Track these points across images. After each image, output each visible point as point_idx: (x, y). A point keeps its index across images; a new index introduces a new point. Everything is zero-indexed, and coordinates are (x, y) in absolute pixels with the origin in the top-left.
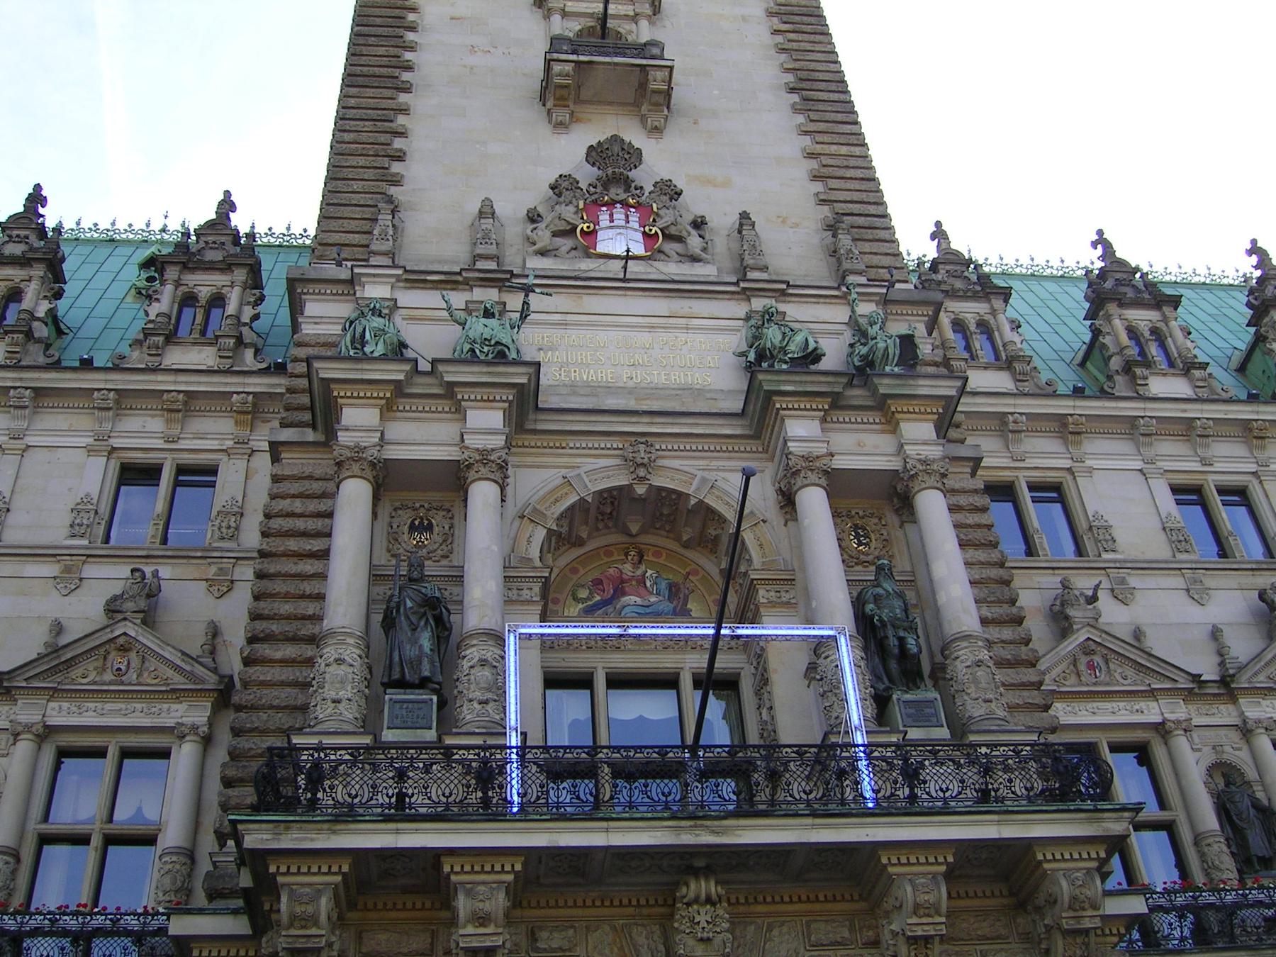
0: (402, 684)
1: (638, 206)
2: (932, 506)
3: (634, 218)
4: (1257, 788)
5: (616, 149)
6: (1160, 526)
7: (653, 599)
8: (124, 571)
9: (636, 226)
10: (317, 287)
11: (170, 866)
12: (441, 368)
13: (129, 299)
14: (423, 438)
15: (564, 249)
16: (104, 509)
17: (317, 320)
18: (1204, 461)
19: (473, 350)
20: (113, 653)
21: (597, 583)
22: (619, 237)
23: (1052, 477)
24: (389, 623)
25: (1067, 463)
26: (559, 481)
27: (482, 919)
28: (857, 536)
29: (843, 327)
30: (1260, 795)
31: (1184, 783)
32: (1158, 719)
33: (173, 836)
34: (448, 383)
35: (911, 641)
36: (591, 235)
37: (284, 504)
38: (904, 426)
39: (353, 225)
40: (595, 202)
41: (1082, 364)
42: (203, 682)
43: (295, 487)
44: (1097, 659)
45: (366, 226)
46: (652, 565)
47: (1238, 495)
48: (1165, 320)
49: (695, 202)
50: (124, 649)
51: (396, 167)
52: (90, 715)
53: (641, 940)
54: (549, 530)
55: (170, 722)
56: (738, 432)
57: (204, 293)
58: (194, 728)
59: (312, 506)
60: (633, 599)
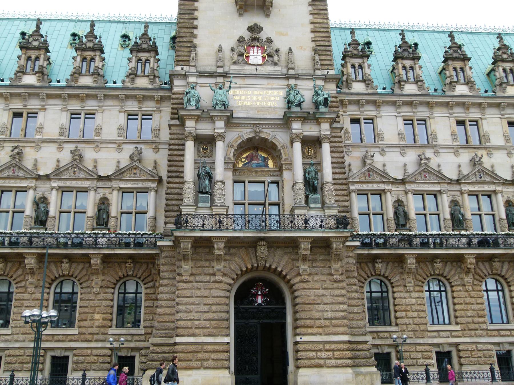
1: (262, 47)
2: (326, 147)
3: (260, 51)
5: (256, 27)
6: (397, 133)
9: (260, 54)
13: (120, 49)
14: (205, 129)
15: (241, 60)
16: (125, 128)
17: (178, 86)
18: (414, 113)
21: (247, 157)
22: (256, 56)
23: (371, 117)
24: (199, 177)
25: (375, 114)
26: (237, 136)
27: (219, 249)
28: (309, 151)
30: (406, 209)
32: (384, 189)
33: (151, 213)
35: (316, 183)
36: (248, 57)
37: (173, 142)
38: (322, 124)
39: (184, 54)
40: (249, 45)
42: (155, 177)
43: (175, 137)
44: (371, 173)
45: (188, 54)
49: (277, 44)
50: (135, 169)
51: (195, 32)
52: (129, 185)
54: (235, 149)
55: (148, 186)
57: (144, 59)
58: (154, 188)
59: (179, 142)
60: (255, 162)
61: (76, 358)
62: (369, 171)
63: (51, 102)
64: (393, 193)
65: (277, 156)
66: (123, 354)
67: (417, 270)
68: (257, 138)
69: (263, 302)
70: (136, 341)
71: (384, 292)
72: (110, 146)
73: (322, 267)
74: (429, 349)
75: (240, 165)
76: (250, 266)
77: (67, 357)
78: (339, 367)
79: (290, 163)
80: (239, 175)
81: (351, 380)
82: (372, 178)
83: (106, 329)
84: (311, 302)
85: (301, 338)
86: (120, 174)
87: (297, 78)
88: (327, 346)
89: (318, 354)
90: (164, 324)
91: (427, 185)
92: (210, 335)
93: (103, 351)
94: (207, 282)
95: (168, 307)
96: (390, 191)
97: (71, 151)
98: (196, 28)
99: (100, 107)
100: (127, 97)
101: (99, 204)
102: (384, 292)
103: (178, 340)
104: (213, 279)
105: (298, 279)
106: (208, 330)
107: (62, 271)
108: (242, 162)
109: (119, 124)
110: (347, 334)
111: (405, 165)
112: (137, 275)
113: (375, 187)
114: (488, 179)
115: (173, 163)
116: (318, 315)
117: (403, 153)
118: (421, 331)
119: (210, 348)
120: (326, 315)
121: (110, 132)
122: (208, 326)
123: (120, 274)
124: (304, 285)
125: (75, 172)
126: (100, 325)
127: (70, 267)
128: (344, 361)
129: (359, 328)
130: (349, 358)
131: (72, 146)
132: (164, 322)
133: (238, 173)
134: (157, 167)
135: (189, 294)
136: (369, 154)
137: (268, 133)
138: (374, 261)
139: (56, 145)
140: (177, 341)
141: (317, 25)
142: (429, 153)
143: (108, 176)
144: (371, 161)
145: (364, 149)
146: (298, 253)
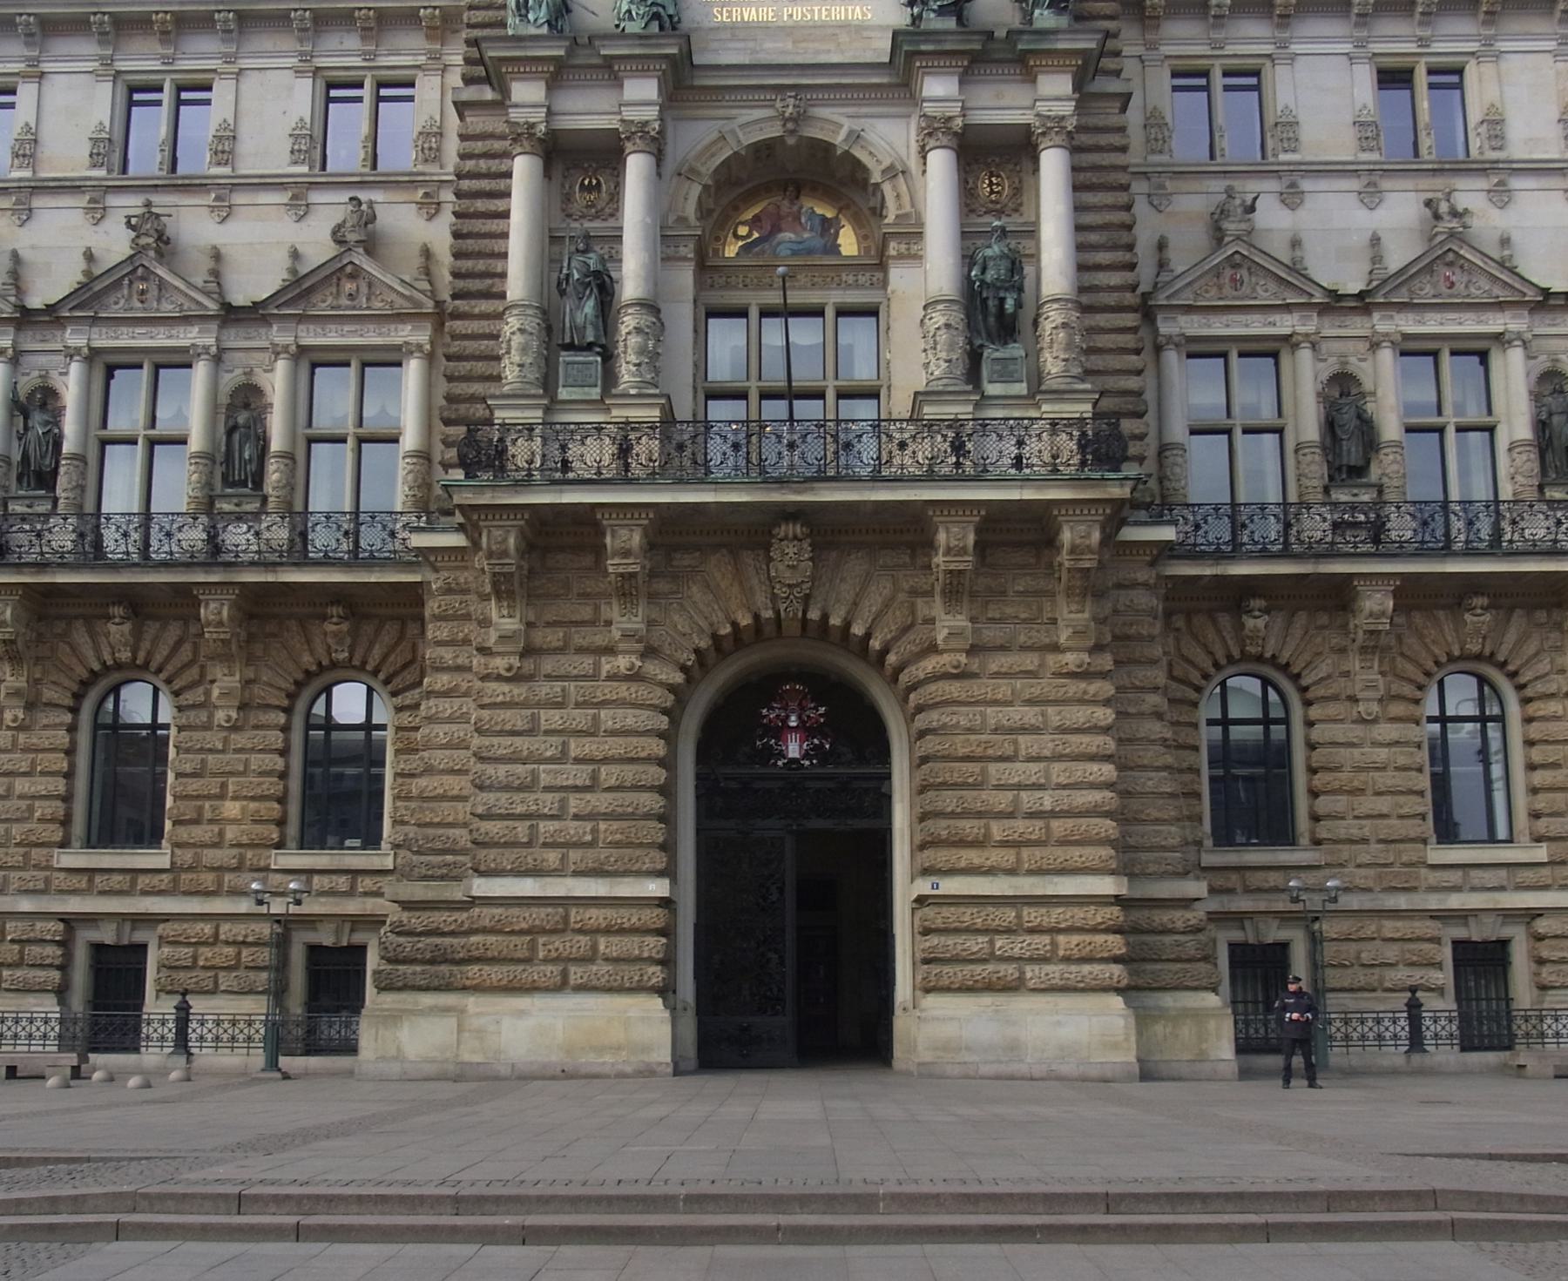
0: (570, 347)
2: (1053, 165)
7: (806, 235)
8: (343, 196)
12: (597, 43)
19: (629, 11)
20: (344, 280)
26: (715, 135)
27: (626, 553)
32: (1287, 331)
34: (605, 56)
35: (1009, 305)
43: (479, 146)
44: (1244, 272)
52: (332, 337)
54: (706, 187)
55: (398, 341)
56: (885, 80)
58: (420, 347)
60: (787, 235)
61: (166, 950)
62: (1236, 266)
63: (62, 46)
64: (1325, 347)
65: (873, 210)
67: (1399, 638)
68: (791, 141)
69: (806, 756)
70: (366, 894)
71: (1277, 721)
73: (1025, 621)
74: (1430, 933)
75: (731, 250)
76: (745, 620)
77: (143, 948)
78: (1075, 990)
79: (913, 233)
80: (727, 286)
81: (1121, 1038)
82: (1246, 289)
83: (265, 852)
84: (979, 751)
85: (935, 886)
88: (1032, 915)
89: (998, 944)
90: (440, 831)
93: (253, 926)
94: (585, 677)
95: (452, 772)
97: (129, 218)
99: (230, 59)
101: (231, 408)
102: (1277, 721)
103: (482, 887)
105: (930, 664)
106: (591, 854)
107: (112, 648)
108: (736, 236)
111: (1375, 241)
112: (364, 663)
113: (1255, 326)
115: (470, 244)
116: (1003, 800)
117: (1371, 196)
118: (1405, 865)
119: (596, 916)
120: (1027, 799)
121: (267, 147)
122: (588, 838)
124: (953, 689)
125: (143, 292)
127: (137, 634)
128: (1096, 968)
129: (1164, 848)
130: (1116, 960)
131: (132, 203)
132: (439, 825)
133: (722, 281)
134: (433, 268)
135: (520, 725)
136: (1238, 202)
138: (1239, 607)
139: (83, 200)
140: (475, 894)
142: (1470, 195)
143: (256, 305)
144: (1243, 226)
145: (1218, 185)
146: (929, 567)
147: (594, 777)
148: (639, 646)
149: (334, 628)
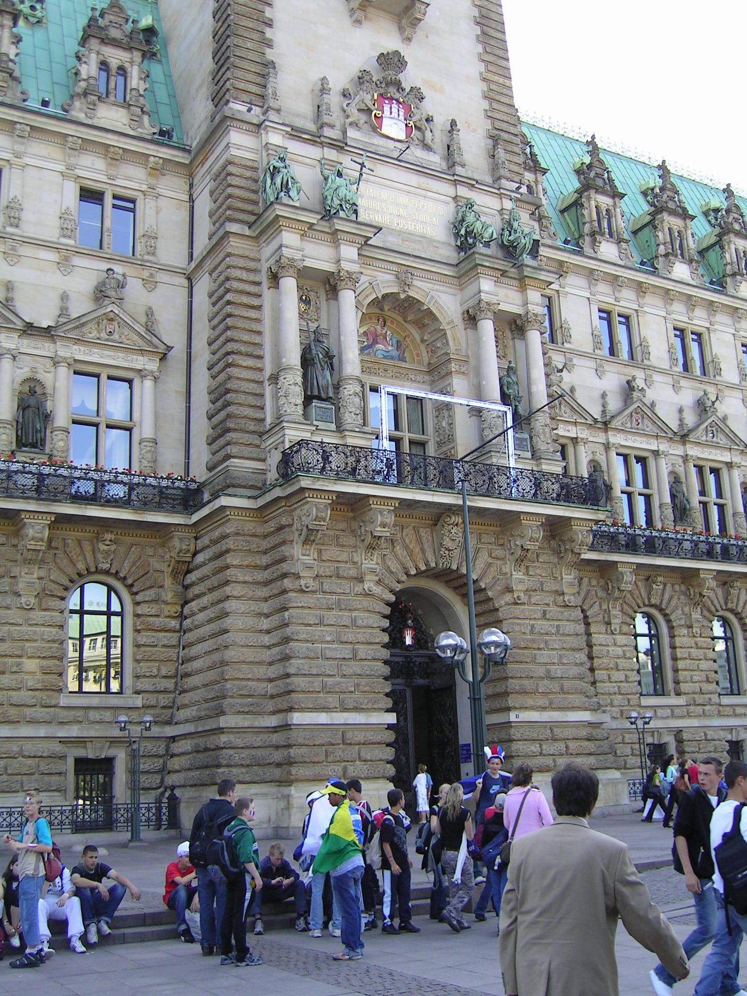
0: (319, 398)
2: (535, 338)
4: (606, 474)
9: (402, 118)
10: (239, 124)
11: (149, 448)
14: (318, 256)
17: (239, 147)
18: (616, 299)
27: (384, 525)
29: (496, 212)
30: (606, 478)
31: (579, 468)
36: (379, 119)
41: (562, 212)
42: (157, 348)
46: (390, 328)
47: (627, 319)
48: (615, 206)
49: (429, 107)
52: (95, 356)
53: (423, 534)
58: (152, 372)
66: (91, 753)
68: (402, 296)
72: (44, 254)
85: (517, 716)
86: (76, 328)
87: (473, 186)
89: (544, 747)
91: (638, 439)
92: (356, 709)
96: (586, 442)
98: (270, 26)
100: (87, 145)
104: (358, 588)
105: (508, 598)
109: (64, 207)
110: (586, 709)
111: (604, 396)
114: (721, 439)
119: (360, 737)
123: (81, 566)
126: (39, 686)
137: (422, 289)
141: (493, 87)
147: (355, 652)
148: (377, 578)
149: (106, 548)
